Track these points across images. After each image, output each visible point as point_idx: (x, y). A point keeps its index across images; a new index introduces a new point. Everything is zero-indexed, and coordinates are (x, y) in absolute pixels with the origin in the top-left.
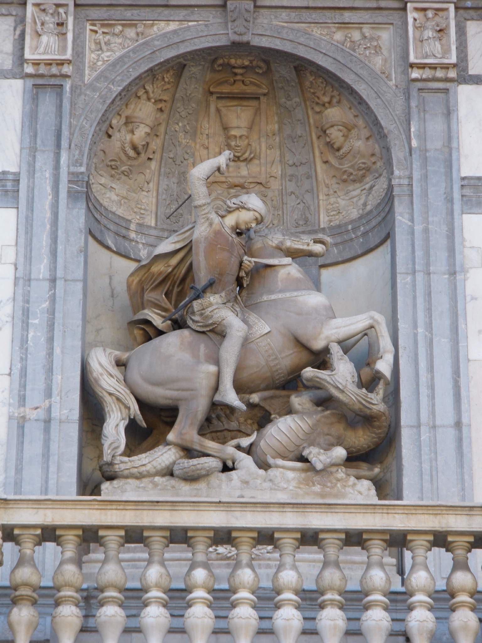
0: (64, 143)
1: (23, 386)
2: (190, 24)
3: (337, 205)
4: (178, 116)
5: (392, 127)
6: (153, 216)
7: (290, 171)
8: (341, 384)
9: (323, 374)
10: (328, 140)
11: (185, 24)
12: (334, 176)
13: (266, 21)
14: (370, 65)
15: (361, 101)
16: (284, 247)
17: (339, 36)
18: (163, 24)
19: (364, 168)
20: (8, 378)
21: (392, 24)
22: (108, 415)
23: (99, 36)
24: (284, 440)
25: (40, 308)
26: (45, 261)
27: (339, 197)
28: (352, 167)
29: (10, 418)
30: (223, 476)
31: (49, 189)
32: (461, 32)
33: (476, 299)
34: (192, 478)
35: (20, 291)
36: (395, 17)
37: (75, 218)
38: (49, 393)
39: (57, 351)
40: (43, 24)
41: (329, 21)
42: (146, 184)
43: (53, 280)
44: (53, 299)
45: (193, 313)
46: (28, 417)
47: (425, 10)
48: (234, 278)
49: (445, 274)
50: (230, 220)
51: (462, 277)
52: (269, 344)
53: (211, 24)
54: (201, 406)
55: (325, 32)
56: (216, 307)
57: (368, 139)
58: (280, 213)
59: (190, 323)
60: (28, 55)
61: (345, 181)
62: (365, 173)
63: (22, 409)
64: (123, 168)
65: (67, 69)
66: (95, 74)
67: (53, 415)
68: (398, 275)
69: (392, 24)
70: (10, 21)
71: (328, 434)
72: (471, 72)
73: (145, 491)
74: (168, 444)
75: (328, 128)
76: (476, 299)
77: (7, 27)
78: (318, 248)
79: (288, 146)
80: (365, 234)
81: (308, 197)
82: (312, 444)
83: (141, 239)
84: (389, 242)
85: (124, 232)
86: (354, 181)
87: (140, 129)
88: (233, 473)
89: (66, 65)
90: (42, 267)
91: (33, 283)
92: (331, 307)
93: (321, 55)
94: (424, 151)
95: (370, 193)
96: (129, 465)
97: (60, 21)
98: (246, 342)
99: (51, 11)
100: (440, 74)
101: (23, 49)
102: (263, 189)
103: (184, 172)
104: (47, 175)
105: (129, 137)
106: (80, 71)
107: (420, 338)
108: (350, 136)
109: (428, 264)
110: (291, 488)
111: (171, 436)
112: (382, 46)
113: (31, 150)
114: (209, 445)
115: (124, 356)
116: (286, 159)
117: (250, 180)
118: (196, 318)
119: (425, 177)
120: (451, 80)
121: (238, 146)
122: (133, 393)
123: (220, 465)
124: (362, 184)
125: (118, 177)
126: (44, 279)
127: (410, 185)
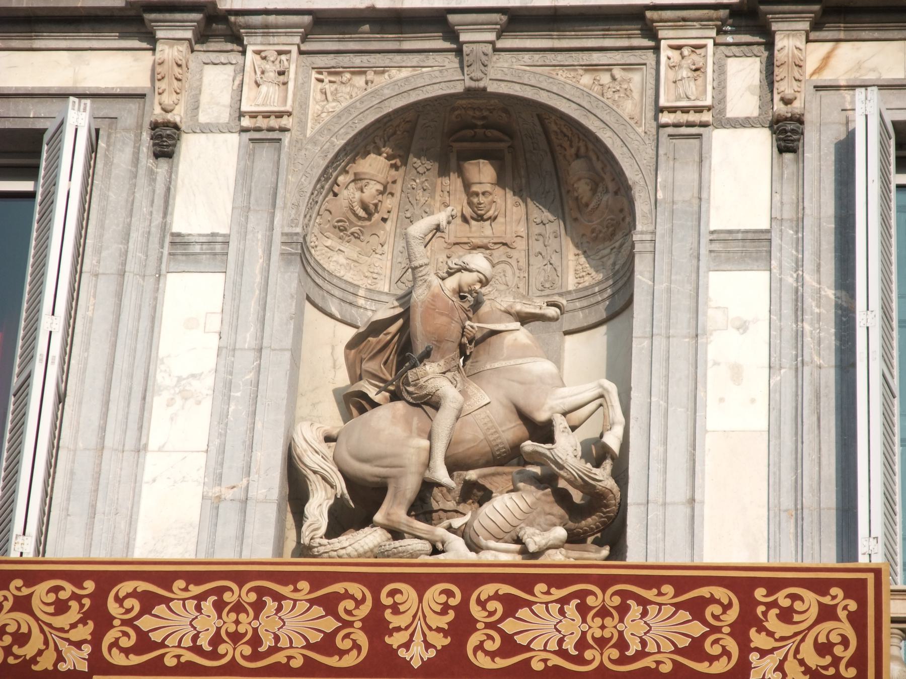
0: (279, 202)
2: (424, 70)
4: (415, 172)
6: (387, 281)
7: (536, 230)
9: (543, 448)
10: (576, 194)
11: (419, 71)
12: (583, 235)
13: (506, 65)
14: (619, 111)
16: (513, 311)
17: (586, 79)
18: (394, 71)
20: (205, 454)
21: (645, 64)
24: (499, 520)
31: (260, 252)
32: (720, 71)
33: (719, 364)
37: (286, 281)
39: (259, 425)
40: (263, 73)
41: (576, 63)
46: (223, 497)
47: (679, 48)
48: (456, 345)
49: (686, 337)
50: (452, 283)
51: (704, 340)
53: (446, 70)
55: (573, 74)
57: (616, 193)
59: (405, 395)
63: (217, 489)
64: (353, 230)
65: (285, 122)
66: (318, 126)
67: (250, 495)
69: (645, 64)
70: (230, 69)
71: (549, 514)
72: (729, 115)
74: (375, 525)
76: (719, 364)
77: (226, 77)
78: (552, 312)
82: (531, 524)
83: (371, 305)
85: (351, 298)
86: (604, 240)
87: (371, 186)
89: (285, 117)
90: (248, 335)
91: (237, 353)
92: (563, 376)
93: (565, 101)
96: (329, 548)
97: (282, 69)
99: (272, 59)
100: (692, 117)
102: (509, 250)
104: (260, 236)
105: (358, 195)
106: (303, 124)
109: (668, 327)
111: (378, 517)
112: (633, 88)
113: (243, 209)
114: (418, 526)
118: (411, 389)
120: (704, 125)
122: (341, 471)
123: (428, 547)
125: (347, 238)
126: (249, 349)
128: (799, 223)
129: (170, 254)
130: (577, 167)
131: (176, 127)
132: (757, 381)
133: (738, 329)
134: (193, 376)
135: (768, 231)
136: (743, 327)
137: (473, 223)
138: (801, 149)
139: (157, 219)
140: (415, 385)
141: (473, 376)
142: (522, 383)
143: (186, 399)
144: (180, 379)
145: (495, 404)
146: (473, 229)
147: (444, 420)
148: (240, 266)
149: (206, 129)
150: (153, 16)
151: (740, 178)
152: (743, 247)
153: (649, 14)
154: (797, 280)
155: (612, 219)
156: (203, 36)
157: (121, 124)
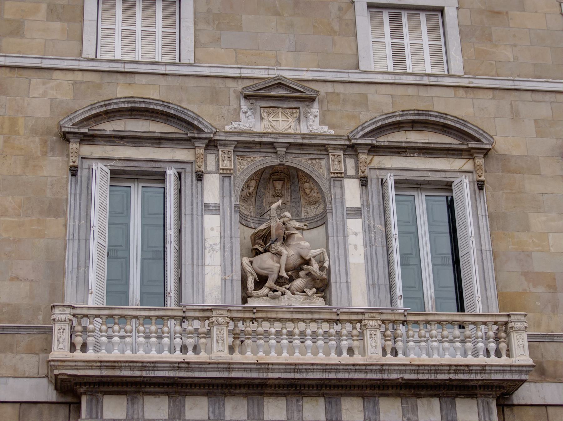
0: (232, 195)
1: (225, 269)
5: (326, 191)
7: (293, 200)
15: (316, 182)
17: (310, 162)
23: (240, 160)
29: (222, 279)
30: (282, 297)
34: (273, 298)
35: (222, 241)
36: (325, 157)
37: (236, 217)
38: (232, 272)
39: (234, 259)
43: (231, 237)
44: (232, 243)
50: (282, 220)
54: (275, 276)
56: (278, 246)
60: (221, 167)
65: (232, 172)
70: (214, 155)
72: (348, 174)
73: (260, 301)
78: (305, 227)
80: (316, 221)
81: (298, 208)
84: (324, 225)
94: (335, 199)
98: (288, 257)
100: (339, 175)
101: (219, 165)
105: (248, 191)
106: (235, 171)
107: (336, 256)
109: (337, 233)
111: (267, 285)
113: (223, 196)
115: (251, 259)
119: (336, 207)
120: (342, 178)
128: (368, 206)
130: (307, 185)
131: (202, 172)
132: (361, 249)
136: (356, 234)
139: (200, 199)
141: (288, 245)
142: (302, 249)
147: (283, 259)
148: (224, 213)
149: (210, 173)
150: (195, 140)
151: (352, 193)
153: (326, 146)
156: (207, 147)
157: (187, 171)
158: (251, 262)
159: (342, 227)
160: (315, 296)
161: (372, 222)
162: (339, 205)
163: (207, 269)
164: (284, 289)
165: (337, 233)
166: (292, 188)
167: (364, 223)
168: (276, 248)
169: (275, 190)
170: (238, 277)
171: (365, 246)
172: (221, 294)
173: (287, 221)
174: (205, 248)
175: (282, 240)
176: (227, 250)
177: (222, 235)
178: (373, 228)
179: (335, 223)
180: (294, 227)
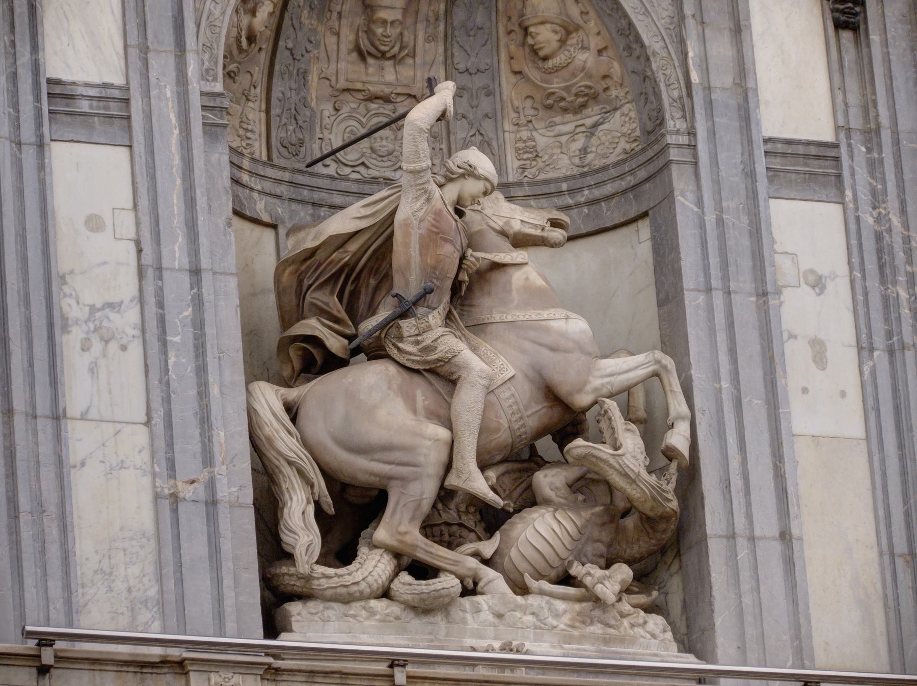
3: (533, 143)
8: (633, 471)
19: (586, 95)
20: (145, 430)
22: (287, 496)
25: (181, 317)
26: (180, 239)
27: (536, 130)
28: (567, 89)
29: (157, 497)
30: (467, 602)
33: (795, 337)
35: (150, 289)
38: (208, 459)
39: (215, 390)
42: (252, 88)
43: (196, 272)
44: (198, 303)
45: (401, 338)
46: (181, 495)
50: (451, 192)
52: (513, 395)
54: (427, 490)
57: (600, 52)
58: (444, 146)
59: (394, 353)
61: (549, 107)
62: (587, 102)
67: (219, 495)
68: (686, 293)
71: (598, 541)
75: (532, 25)
76: (795, 337)
79: (459, 40)
80: (591, 203)
81: (487, 125)
86: (565, 110)
88: (478, 598)
90: (177, 249)
91: (166, 275)
95: (592, 134)
103: (305, 72)
104: (169, 94)
108: (569, 42)
109: (726, 278)
110: (562, 626)
116: (456, 60)
117: (399, 90)
121: (388, 37)
124: (579, 116)
126: (180, 270)
127: (693, 147)
129: (50, 112)
133: (813, 287)
134: (111, 305)
135: (835, 146)
137: (370, 61)
138: (862, 27)
139: (24, 56)
140: (417, 343)
141: (478, 328)
142: (553, 349)
143: (107, 342)
144: (93, 309)
145: (520, 377)
146: (371, 70)
147: (468, 403)
152: (806, 165)
154: (878, 220)
155: (590, 87)
158: (292, 411)
159: (746, 242)
160: (626, 607)
161: (896, 221)
162: (727, 122)
163: (81, 440)
164: (473, 563)
165: (726, 278)
166: (459, 15)
167: (852, 227)
168: (428, 339)
169: (370, 20)
170: (237, 486)
171: (864, 348)
172: (160, 579)
173: (475, 200)
174: (65, 328)
175: (447, 297)
176: (174, 339)
177: (148, 256)
178: (900, 256)
179: (710, 218)
180: (503, 233)
